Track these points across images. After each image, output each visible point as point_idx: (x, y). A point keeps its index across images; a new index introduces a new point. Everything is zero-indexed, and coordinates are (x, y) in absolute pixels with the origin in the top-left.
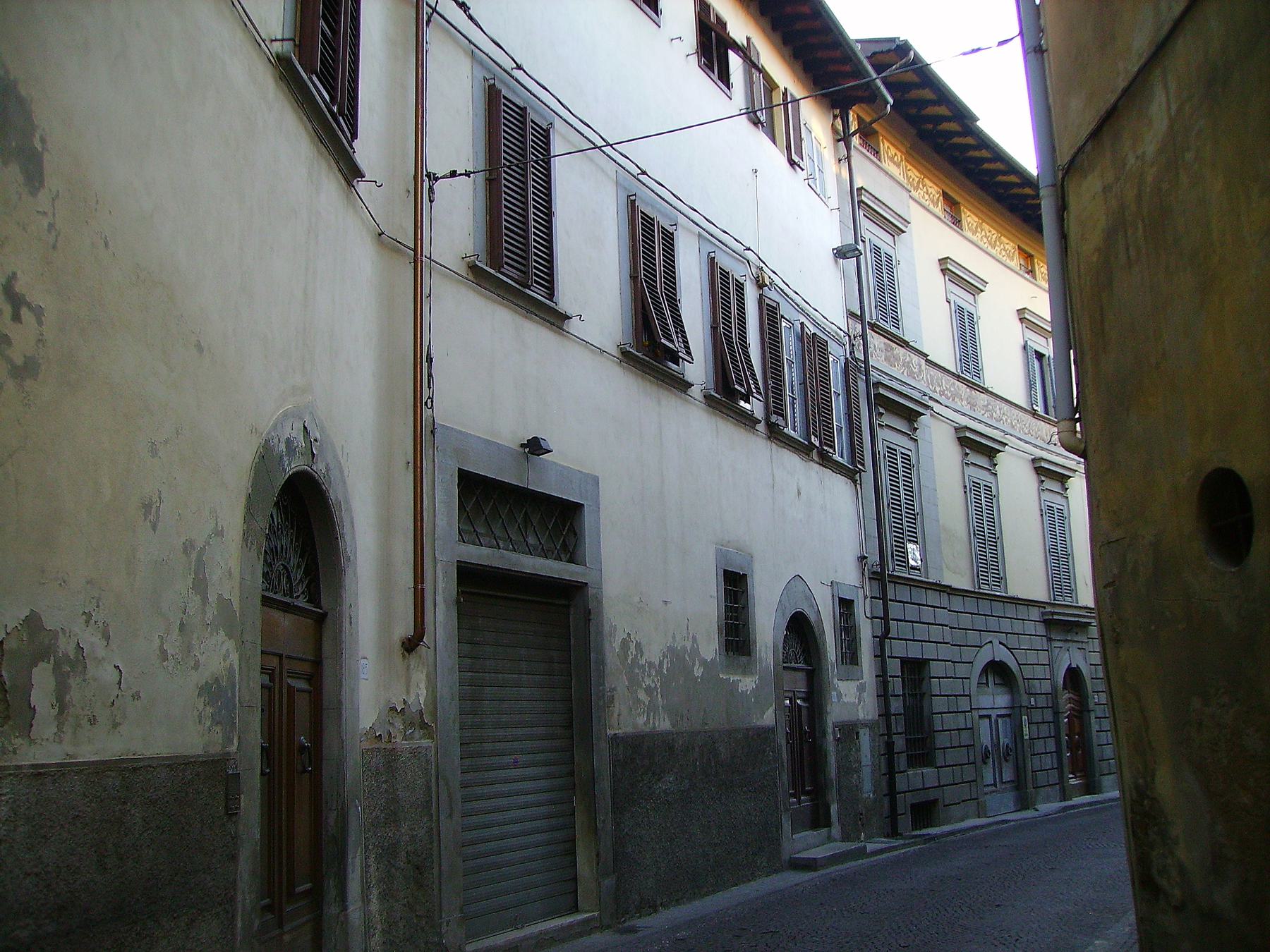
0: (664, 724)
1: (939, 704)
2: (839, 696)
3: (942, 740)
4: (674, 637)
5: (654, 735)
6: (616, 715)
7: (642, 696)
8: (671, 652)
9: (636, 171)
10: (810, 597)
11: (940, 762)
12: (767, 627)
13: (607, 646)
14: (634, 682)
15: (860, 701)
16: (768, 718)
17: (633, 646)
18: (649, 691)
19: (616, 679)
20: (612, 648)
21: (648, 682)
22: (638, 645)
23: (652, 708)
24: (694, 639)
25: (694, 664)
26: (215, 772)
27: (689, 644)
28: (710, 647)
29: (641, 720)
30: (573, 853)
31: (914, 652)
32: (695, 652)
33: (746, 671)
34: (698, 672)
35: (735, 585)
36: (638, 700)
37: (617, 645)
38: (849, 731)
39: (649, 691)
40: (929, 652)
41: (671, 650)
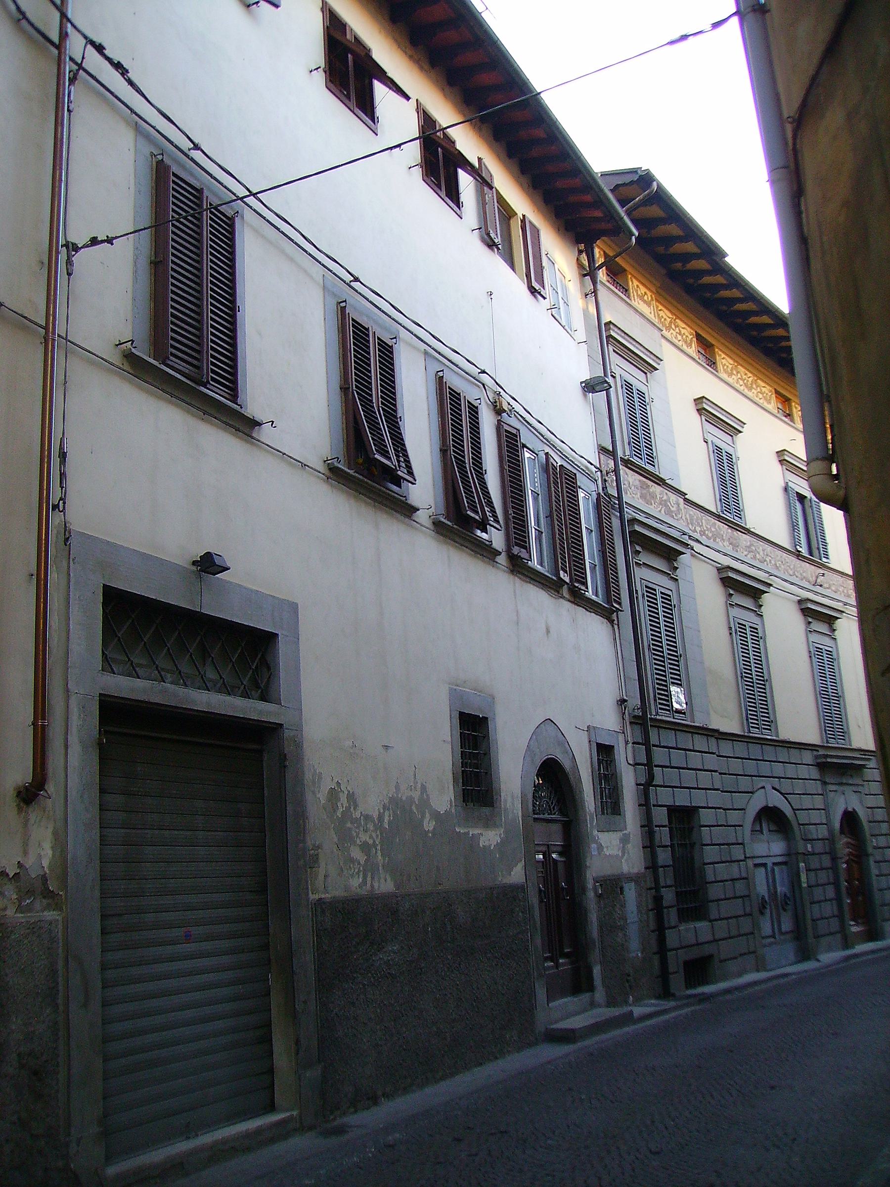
0: (385, 885)
1: (710, 854)
2: (600, 848)
3: (715, 892)
4: (397, 787)
5: (372, 899)
6: (321, 877)
7: (356, 854)
8: (394, 803)
10: (563, 742)
11: (714, 914)
12: (513, 774)
13: (309, 796)
14: (345, 838)
16: (517, 874)
18: (365, 848)
19: (320, 833)
20: (316, 801)
21: (364, 837)
22: (351, 797)
23: (369, 868)
24: (424, 788)
25: (423, 816)
27: (416, 795)
28: (444, 797)
29: (355, 882)
30: (267, 1040)
31: (682, 799)
32: (425, 803)
33: (489, 823)
34: (429, 825)
35: (473, 730)
36: (352, 860)
37: (322, 796)
38: (612, 886)
39: (365, 848)
40: (698, 798)
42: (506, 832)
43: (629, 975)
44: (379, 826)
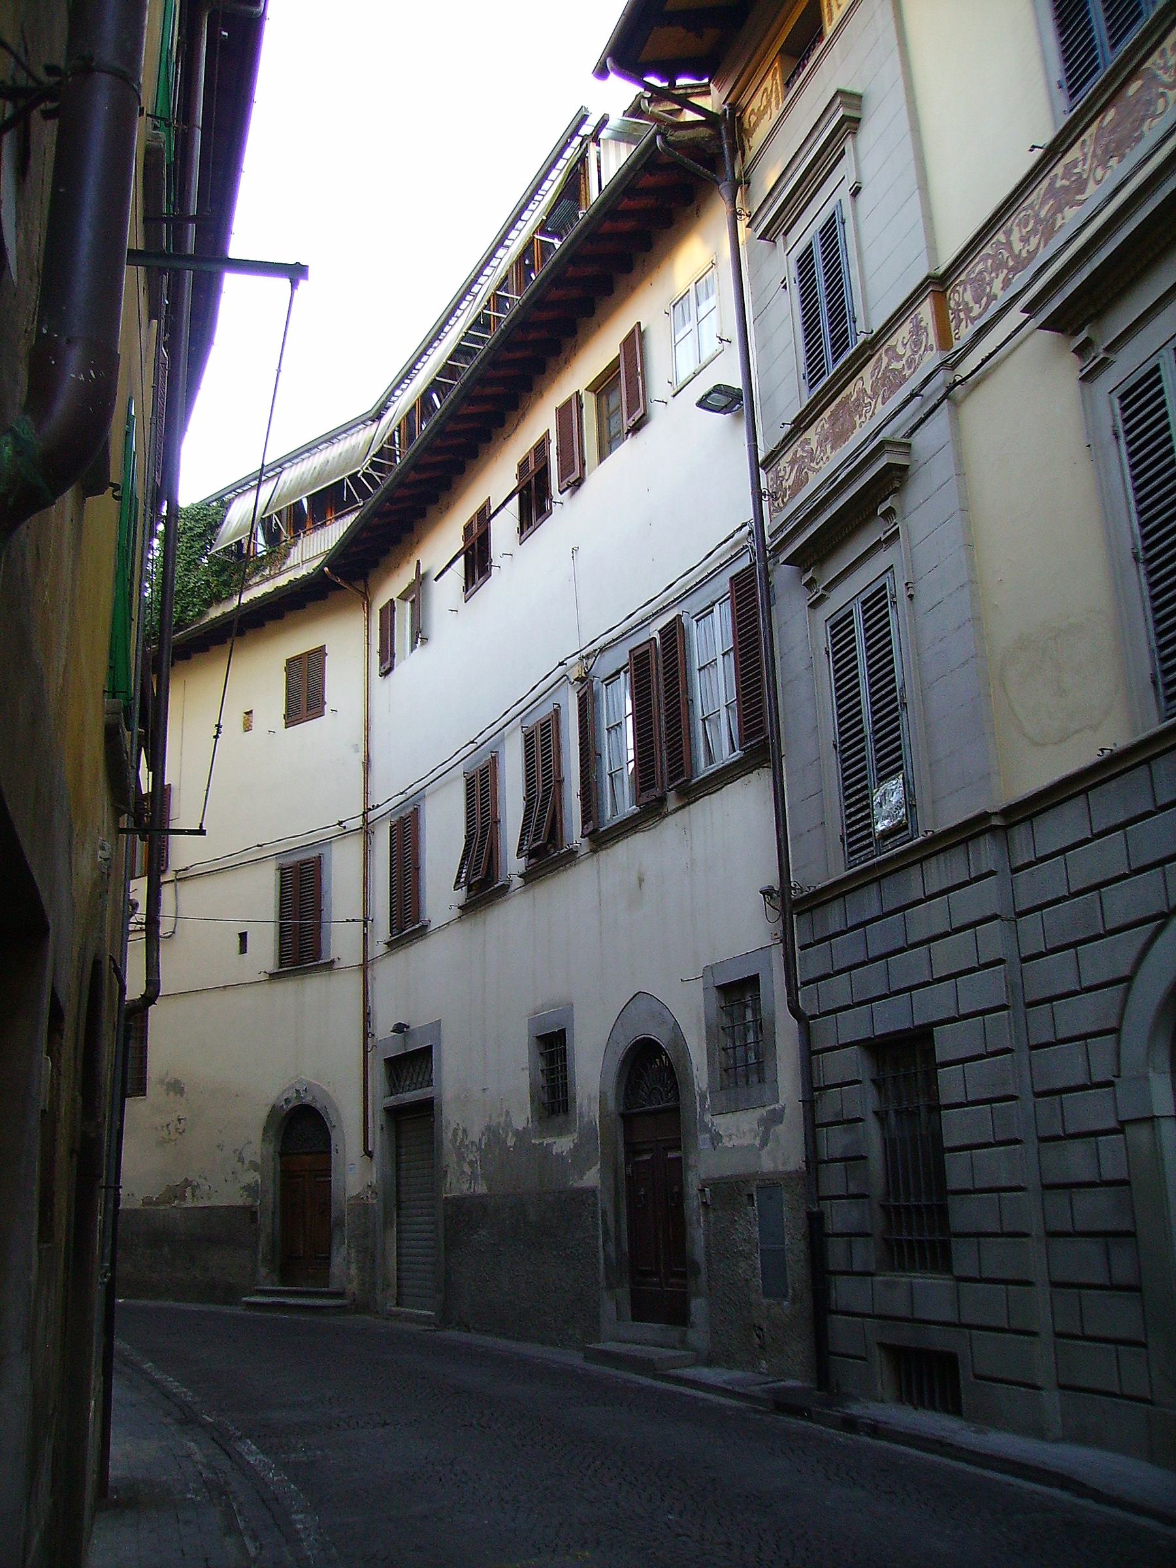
0: (481, 1189)
1: (957, 1127)
2: (716, 1138)
3: (965, 1214)
7: (467, 1168)
9: (473, 746)
10: (660, 1011)
11: (964, 1263)
12: (591, 1073)
14: (461, 1157)
15: (764, 1143)
16: (592, 1178)
17: (460, 1133)
18: (471, 1163)
19: (450, 1159)
20: (448, 1136)
21: (471, 1157)
22: (464, 1131)
23: (473, 1177)
24: (508, 1112)
26: (250, 1213)
28: (522, 1116)
31: (891, 1018)
32: (509, 1124)
34: (511, 1142)
35: (553, 1046)
37: (450, 1134)
38: (729, 1192)
39: (471, 1163)
40: (932, 1005)
41: (488, 1128)
42: (580, 1137)
43: (761, 1329)
44: (479, 1149)
